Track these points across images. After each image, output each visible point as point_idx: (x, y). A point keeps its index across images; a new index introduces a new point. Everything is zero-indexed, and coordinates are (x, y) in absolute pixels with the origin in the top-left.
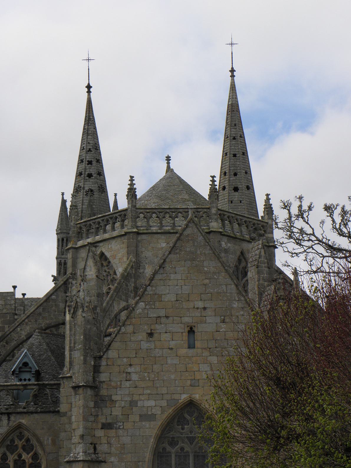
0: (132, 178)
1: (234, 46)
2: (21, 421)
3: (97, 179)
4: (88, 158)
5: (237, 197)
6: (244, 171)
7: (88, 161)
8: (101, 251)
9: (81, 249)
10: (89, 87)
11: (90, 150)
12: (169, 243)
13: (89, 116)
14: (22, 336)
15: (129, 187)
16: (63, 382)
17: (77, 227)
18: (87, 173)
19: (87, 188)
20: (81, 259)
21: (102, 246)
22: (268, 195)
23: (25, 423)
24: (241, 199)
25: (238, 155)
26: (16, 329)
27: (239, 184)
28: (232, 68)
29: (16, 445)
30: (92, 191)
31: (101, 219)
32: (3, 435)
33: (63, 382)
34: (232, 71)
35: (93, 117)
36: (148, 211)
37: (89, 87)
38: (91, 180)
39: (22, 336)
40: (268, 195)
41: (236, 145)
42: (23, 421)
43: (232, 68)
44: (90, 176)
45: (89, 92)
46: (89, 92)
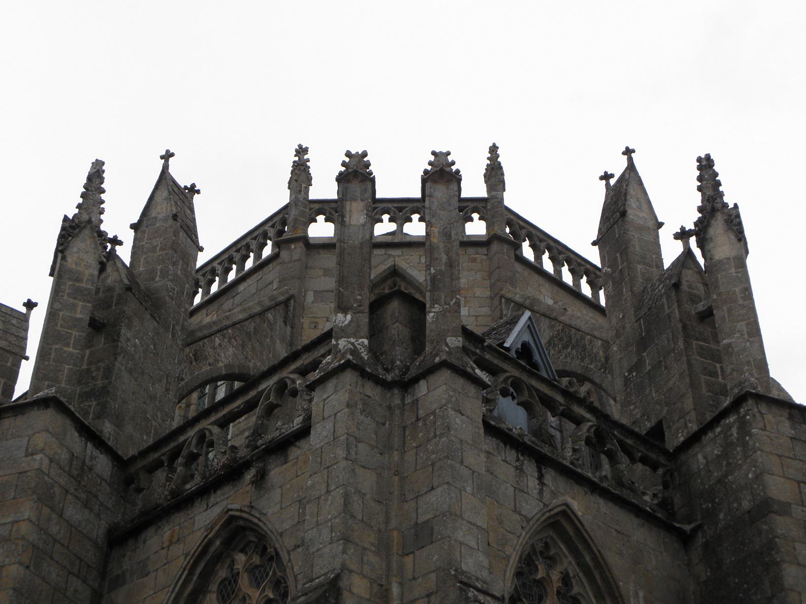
0: (494, 149)
2: (570, 500)
8: (394, 265)
9: (321, 251)
12: (557, 302)
14: (221, 364)
15: (489, 162)
16: (760, 412)
17: (311, 209)
20: (321, 272)
21: (398, 256)
23: (579, 514)
26: (213, 337)
29: (539, 583)
31: (396, 205)
32: (531, 523)
33: (760, 412)
36: (521, 223)
39: (221, 364)
42: (575, 505)
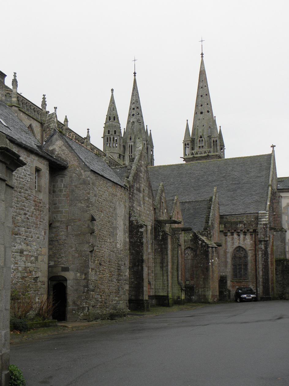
1: (203, 42)
3: (136, 116)
4: (133, 107)
5: (202, 116)
6: (206, 103)
7: (133, 108)
10: (135, 73)
11: (134, 103)
13: (134, 88)
18: (132, 114)
19: (131, 121)
22: (15, 73)
24: (204, 118)
25: (203, 96)
27: (203, 110)
28: (202, 53)
30: (134, 122)
34: (202, 54)
35: (137, 87)
37: (135, 73)
38: (134, 117)
40: (15, 73)
41: (203, 91)
43: (202, 53)
44: (133, 115)
45: (135, 76)
46: (135, 76)
